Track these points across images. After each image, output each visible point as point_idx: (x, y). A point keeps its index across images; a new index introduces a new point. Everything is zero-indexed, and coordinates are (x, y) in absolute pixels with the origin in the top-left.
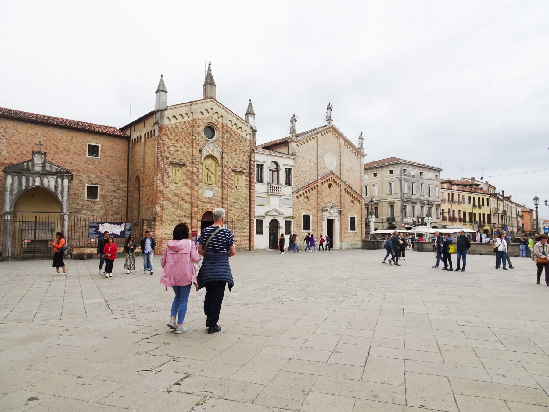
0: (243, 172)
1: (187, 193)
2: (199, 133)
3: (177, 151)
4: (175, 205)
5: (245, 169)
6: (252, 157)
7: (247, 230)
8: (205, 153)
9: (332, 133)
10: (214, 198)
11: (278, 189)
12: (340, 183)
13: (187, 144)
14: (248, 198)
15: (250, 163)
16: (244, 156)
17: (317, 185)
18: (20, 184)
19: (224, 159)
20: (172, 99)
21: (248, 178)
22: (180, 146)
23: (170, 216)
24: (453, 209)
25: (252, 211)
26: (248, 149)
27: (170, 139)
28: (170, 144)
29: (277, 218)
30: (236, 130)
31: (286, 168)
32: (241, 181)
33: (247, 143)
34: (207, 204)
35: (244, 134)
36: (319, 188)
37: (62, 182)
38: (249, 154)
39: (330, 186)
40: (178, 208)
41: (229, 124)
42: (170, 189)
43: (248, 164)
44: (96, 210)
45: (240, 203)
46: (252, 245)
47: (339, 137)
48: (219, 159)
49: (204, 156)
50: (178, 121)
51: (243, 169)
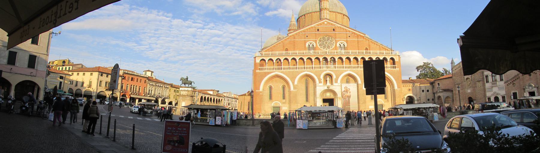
0: (480, 81)
3: (458, 79)
10: (471, 92)
11: (496, 84)
17: (519, 77)
29: (497, 96)
32: (479, 84)
45: (481, 92)
48: (470, 78)
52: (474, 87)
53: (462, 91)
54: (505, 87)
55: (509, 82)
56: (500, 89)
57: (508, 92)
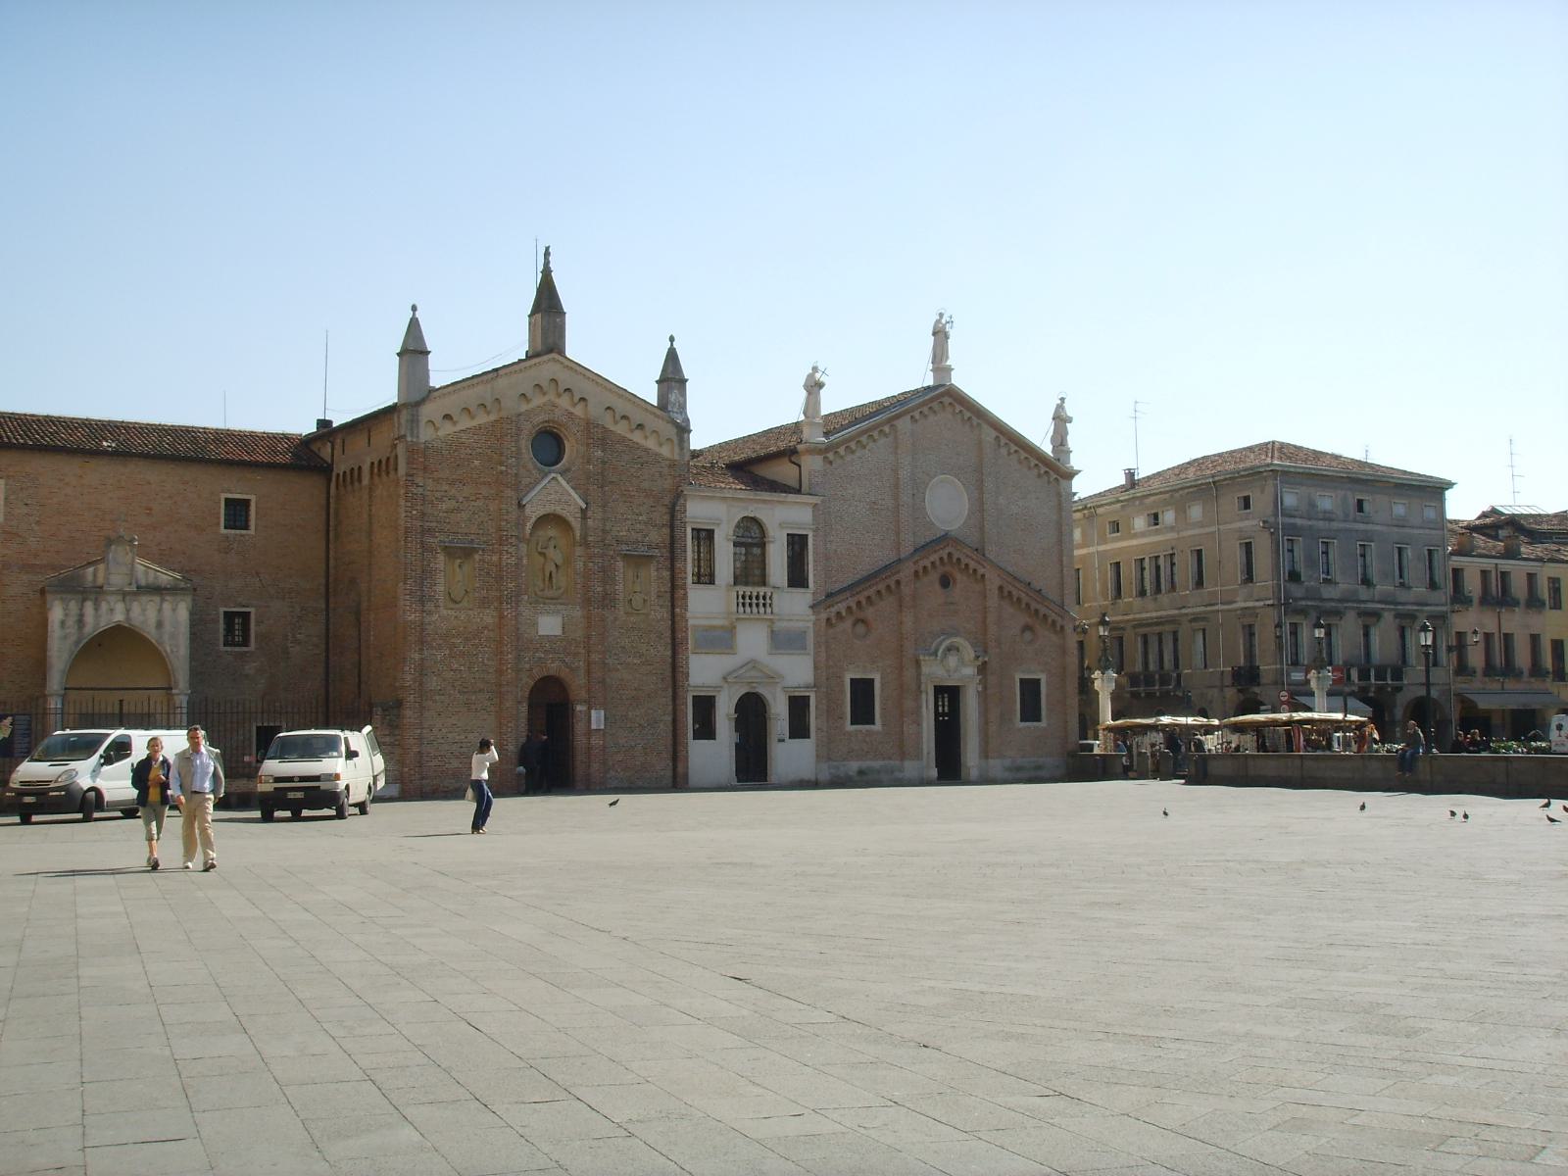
1: (486, 627)
2: (518, 454)
3: (458, 510)
4: (453, 660)
5: (658, 547)
6: (677, 508)
7: (664, 727)
8: (533, 512)
9: (949, 409)
11: (764, 602)
12: (981, 571)
13: (485, 491)
14: (668, 634)
15: (672, 527)
16: (653, 509)
17: (898, 583)
18: (81, 622)
19: (590, 522)
20: (440, 375)
21: (666, 574)
22: (464, 495)
23: (441, 692)
24: (1504, 631)
25: (681, 669)
26: (665, 486)
27: (437, 480)
28: (438, 495)
29: (761, 690)
30: (629, 436)
31: (788, 535)
33: (661, 469)
34: (543, 656)
35: (651, 444)
36: (906, 590)
37: (174, 610)
38: (667, 501)
39: (945, 582)
40: (462, 668)
41: (607, 421)
42: (443, 617)
43: (666, 531)
44: (247, 676)
46: (680, 769)
47: (975, 421)
49: (533, 519)
50: (459, 427)
51: (650, 547)
52: (598, 601)
53: (489, 620)
54: (817, 634)
55: (841, 607)
56: (783, 641)
57: (825, 672)
